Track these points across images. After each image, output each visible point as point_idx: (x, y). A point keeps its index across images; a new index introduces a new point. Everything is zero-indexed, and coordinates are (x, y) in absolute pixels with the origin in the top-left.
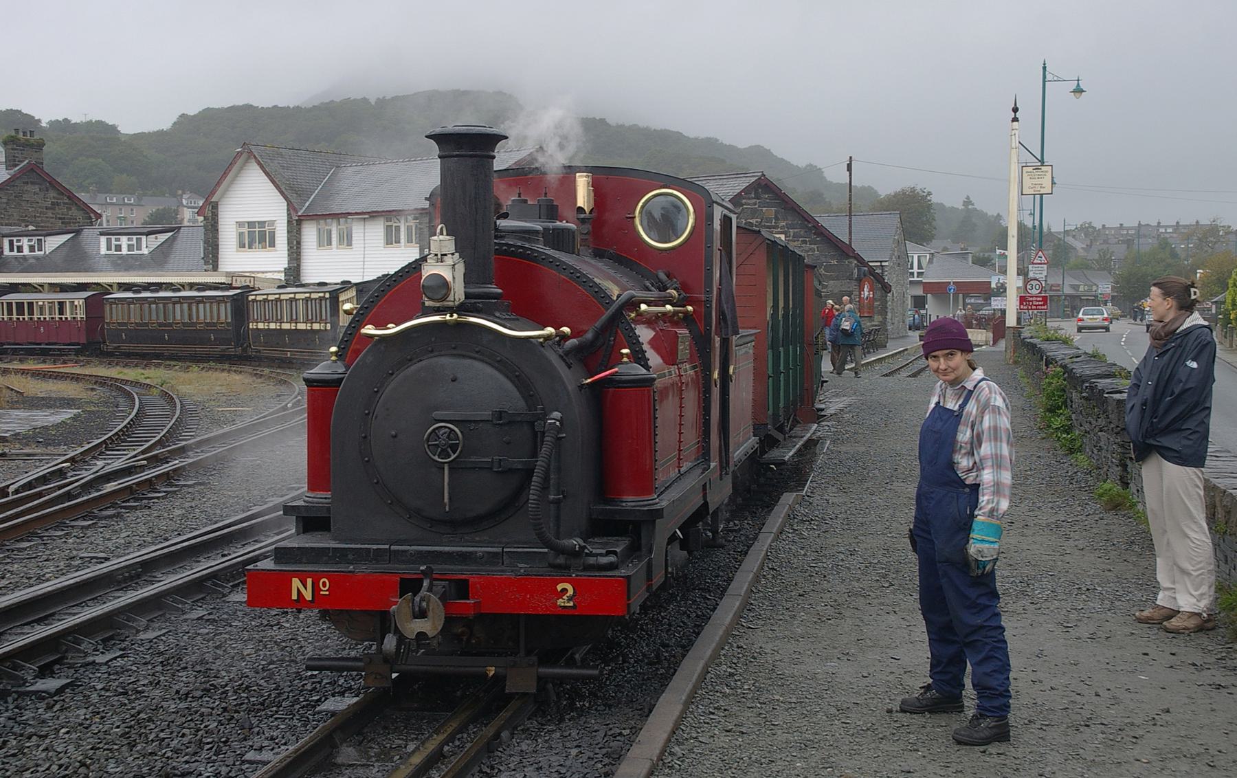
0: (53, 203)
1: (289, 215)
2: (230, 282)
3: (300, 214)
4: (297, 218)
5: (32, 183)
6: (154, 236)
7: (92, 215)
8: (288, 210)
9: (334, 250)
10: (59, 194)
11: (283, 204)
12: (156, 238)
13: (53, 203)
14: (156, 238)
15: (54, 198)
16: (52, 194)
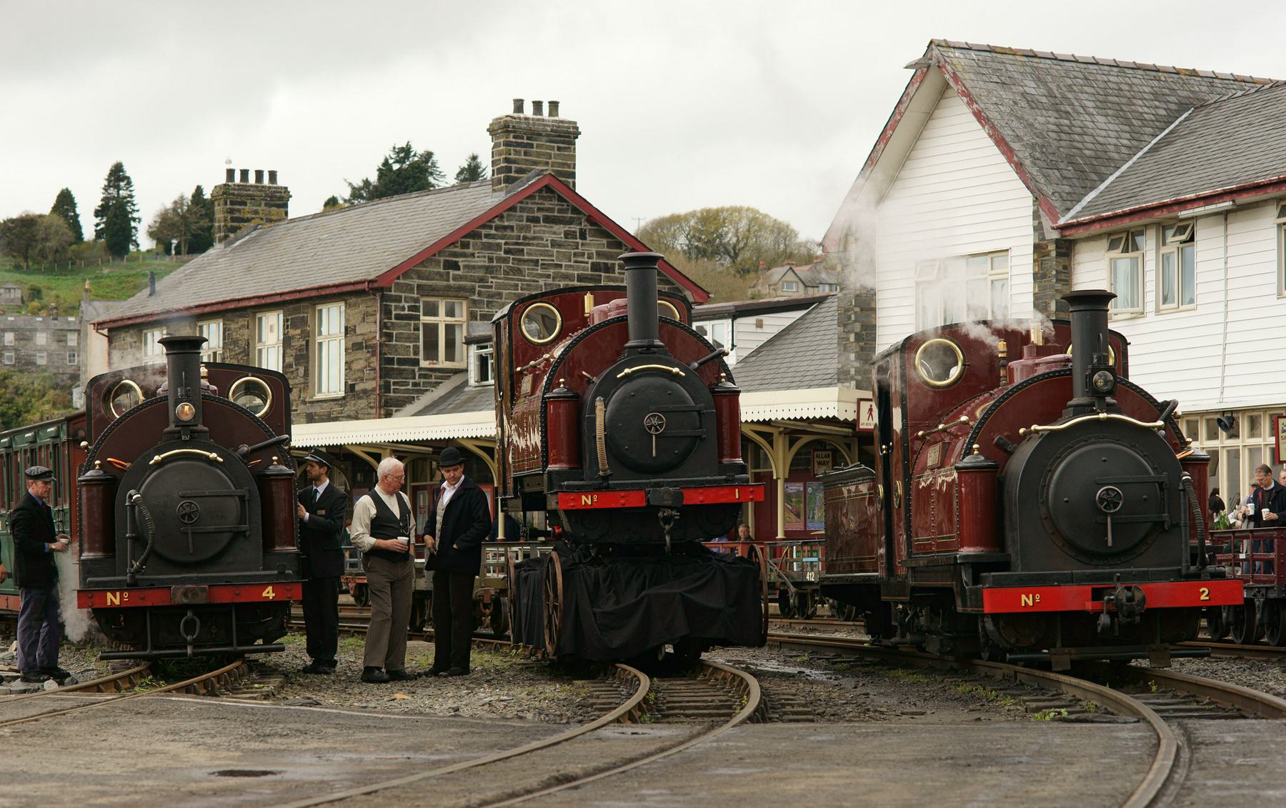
0: (595, 267)
1: (1038, 229)
2: (851, 417)
3: (1062, 221)
4: (1055, 235)
5: (549, 220)
6: (752, 320)
7: (689, 295)
8: (1036, 215)
9: (1151, 316)
10: (609, 245)
11: (1026, 200)
12: (760, 325)
13: (595, 267)
14: (760, 325)
15: (599, 254)
16: (595, 246)
